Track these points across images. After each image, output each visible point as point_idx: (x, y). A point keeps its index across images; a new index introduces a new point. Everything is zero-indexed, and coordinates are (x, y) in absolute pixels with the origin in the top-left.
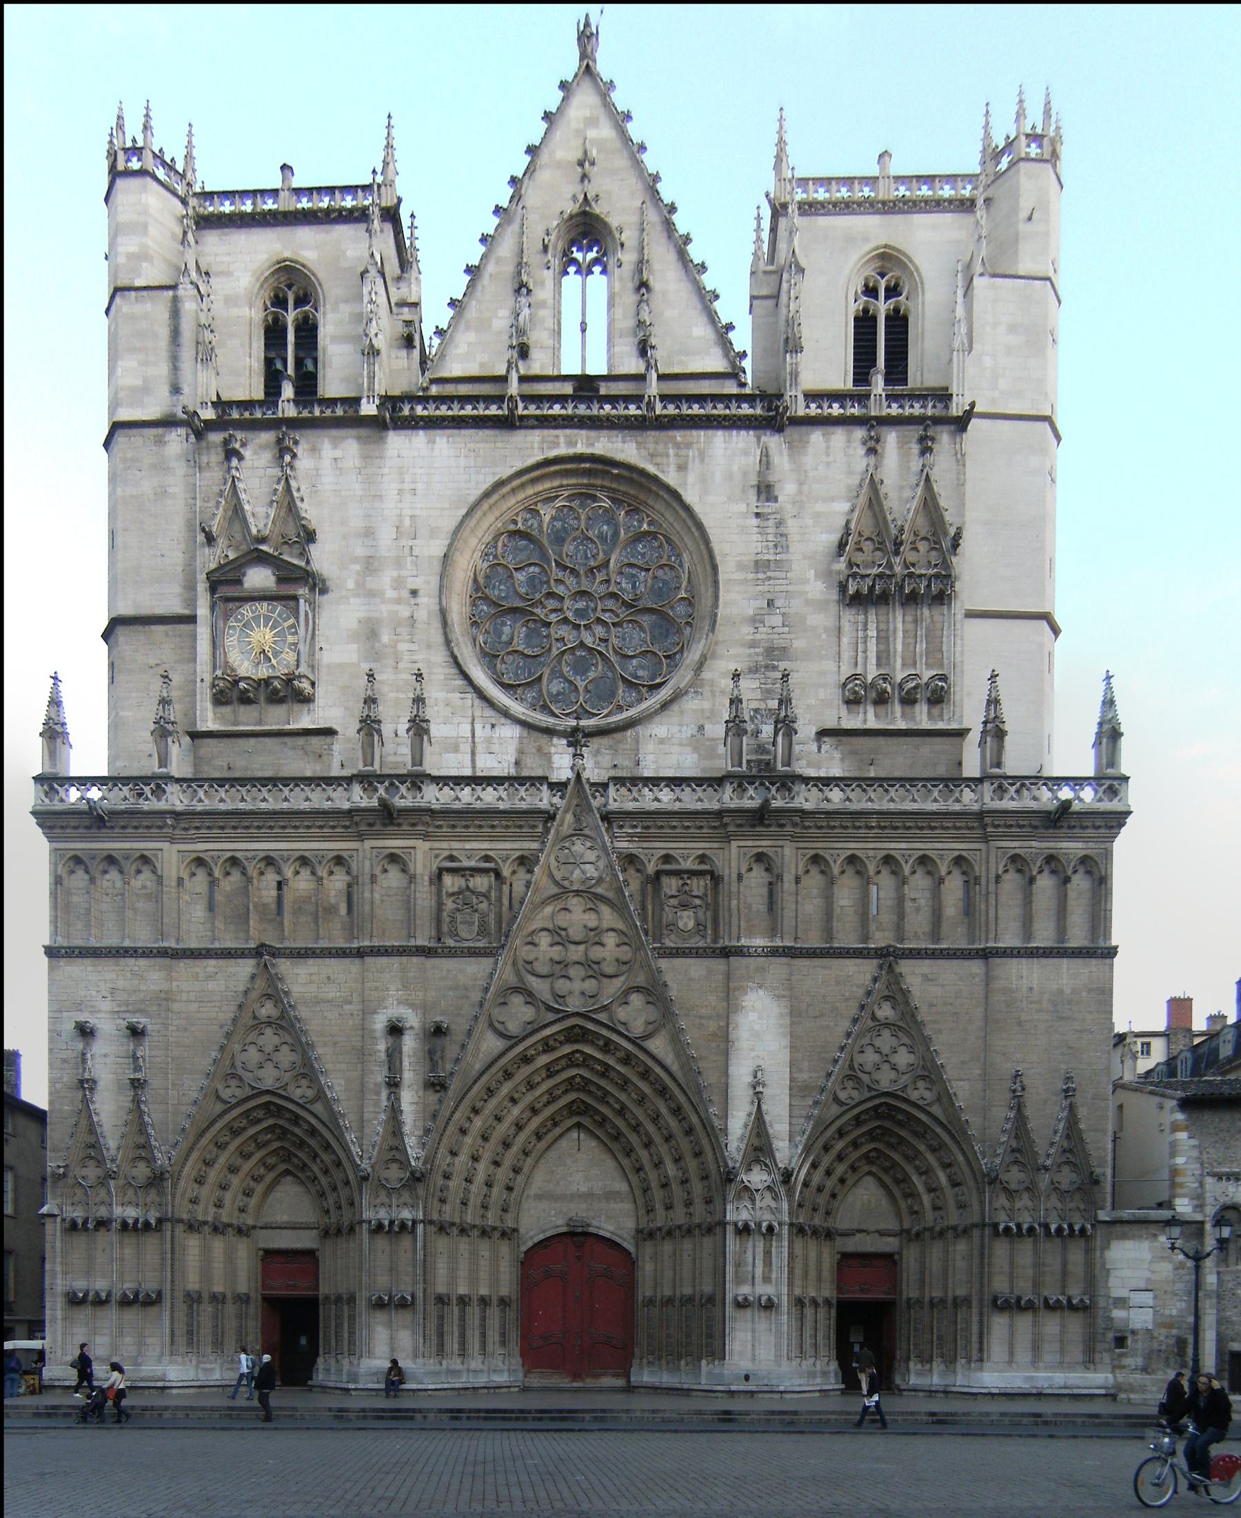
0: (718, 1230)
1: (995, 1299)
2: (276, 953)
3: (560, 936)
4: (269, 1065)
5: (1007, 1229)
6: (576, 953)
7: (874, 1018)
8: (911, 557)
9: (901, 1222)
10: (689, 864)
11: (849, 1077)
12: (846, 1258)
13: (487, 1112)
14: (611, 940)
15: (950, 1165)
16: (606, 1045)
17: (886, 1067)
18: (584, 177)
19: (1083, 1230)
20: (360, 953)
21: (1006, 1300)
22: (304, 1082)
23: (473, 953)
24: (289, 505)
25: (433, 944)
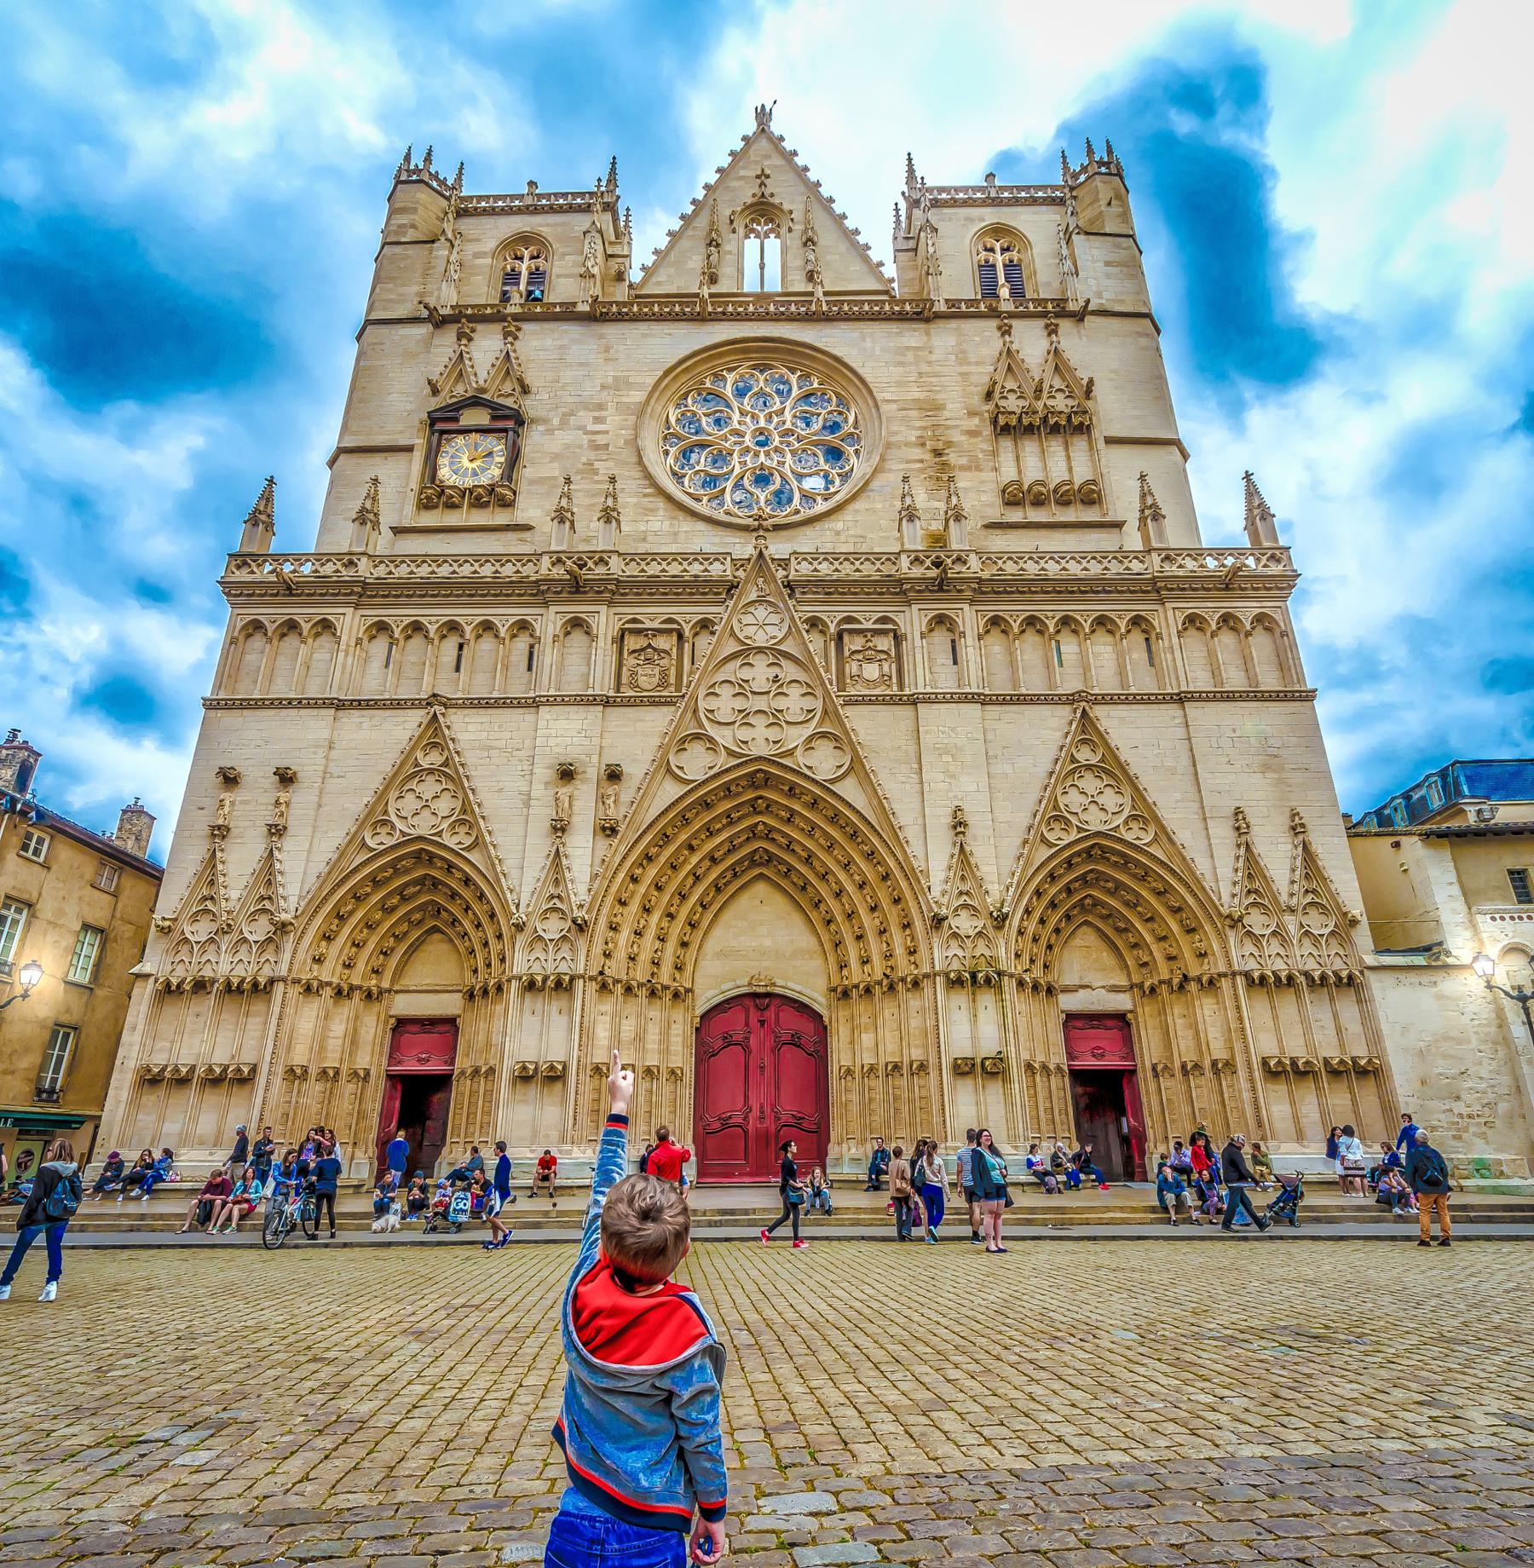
0: (925, 983)
1: (1265, 1062)
2: (448, 704)
3: (742, 689)
4: (426, 813)
5: (1263, 978)
6: (760, 703)
7: (1073, 760)
8: (1050, 402)
9: (1129, 974)
10: (869, 625)
11: (1056, 818)
12: (1072, 1020)
13: (662, 859)
14: (795, 691)
15: (1179, 909)
16: (790, 790)
17: (1093, 807)
18: (762, 184)
19: (1350, 977)
20: (535, 704)
21: (1280, 1062)
22: (463, 830)
23: (655, 702)
24: (506, 364)
25: (611, 693)
